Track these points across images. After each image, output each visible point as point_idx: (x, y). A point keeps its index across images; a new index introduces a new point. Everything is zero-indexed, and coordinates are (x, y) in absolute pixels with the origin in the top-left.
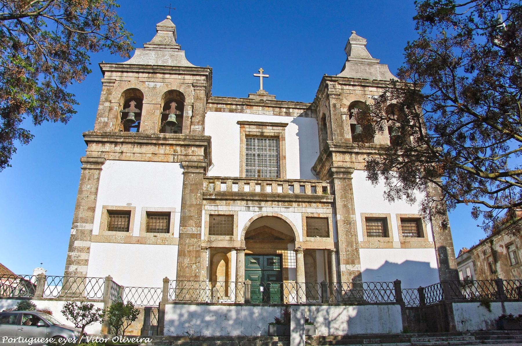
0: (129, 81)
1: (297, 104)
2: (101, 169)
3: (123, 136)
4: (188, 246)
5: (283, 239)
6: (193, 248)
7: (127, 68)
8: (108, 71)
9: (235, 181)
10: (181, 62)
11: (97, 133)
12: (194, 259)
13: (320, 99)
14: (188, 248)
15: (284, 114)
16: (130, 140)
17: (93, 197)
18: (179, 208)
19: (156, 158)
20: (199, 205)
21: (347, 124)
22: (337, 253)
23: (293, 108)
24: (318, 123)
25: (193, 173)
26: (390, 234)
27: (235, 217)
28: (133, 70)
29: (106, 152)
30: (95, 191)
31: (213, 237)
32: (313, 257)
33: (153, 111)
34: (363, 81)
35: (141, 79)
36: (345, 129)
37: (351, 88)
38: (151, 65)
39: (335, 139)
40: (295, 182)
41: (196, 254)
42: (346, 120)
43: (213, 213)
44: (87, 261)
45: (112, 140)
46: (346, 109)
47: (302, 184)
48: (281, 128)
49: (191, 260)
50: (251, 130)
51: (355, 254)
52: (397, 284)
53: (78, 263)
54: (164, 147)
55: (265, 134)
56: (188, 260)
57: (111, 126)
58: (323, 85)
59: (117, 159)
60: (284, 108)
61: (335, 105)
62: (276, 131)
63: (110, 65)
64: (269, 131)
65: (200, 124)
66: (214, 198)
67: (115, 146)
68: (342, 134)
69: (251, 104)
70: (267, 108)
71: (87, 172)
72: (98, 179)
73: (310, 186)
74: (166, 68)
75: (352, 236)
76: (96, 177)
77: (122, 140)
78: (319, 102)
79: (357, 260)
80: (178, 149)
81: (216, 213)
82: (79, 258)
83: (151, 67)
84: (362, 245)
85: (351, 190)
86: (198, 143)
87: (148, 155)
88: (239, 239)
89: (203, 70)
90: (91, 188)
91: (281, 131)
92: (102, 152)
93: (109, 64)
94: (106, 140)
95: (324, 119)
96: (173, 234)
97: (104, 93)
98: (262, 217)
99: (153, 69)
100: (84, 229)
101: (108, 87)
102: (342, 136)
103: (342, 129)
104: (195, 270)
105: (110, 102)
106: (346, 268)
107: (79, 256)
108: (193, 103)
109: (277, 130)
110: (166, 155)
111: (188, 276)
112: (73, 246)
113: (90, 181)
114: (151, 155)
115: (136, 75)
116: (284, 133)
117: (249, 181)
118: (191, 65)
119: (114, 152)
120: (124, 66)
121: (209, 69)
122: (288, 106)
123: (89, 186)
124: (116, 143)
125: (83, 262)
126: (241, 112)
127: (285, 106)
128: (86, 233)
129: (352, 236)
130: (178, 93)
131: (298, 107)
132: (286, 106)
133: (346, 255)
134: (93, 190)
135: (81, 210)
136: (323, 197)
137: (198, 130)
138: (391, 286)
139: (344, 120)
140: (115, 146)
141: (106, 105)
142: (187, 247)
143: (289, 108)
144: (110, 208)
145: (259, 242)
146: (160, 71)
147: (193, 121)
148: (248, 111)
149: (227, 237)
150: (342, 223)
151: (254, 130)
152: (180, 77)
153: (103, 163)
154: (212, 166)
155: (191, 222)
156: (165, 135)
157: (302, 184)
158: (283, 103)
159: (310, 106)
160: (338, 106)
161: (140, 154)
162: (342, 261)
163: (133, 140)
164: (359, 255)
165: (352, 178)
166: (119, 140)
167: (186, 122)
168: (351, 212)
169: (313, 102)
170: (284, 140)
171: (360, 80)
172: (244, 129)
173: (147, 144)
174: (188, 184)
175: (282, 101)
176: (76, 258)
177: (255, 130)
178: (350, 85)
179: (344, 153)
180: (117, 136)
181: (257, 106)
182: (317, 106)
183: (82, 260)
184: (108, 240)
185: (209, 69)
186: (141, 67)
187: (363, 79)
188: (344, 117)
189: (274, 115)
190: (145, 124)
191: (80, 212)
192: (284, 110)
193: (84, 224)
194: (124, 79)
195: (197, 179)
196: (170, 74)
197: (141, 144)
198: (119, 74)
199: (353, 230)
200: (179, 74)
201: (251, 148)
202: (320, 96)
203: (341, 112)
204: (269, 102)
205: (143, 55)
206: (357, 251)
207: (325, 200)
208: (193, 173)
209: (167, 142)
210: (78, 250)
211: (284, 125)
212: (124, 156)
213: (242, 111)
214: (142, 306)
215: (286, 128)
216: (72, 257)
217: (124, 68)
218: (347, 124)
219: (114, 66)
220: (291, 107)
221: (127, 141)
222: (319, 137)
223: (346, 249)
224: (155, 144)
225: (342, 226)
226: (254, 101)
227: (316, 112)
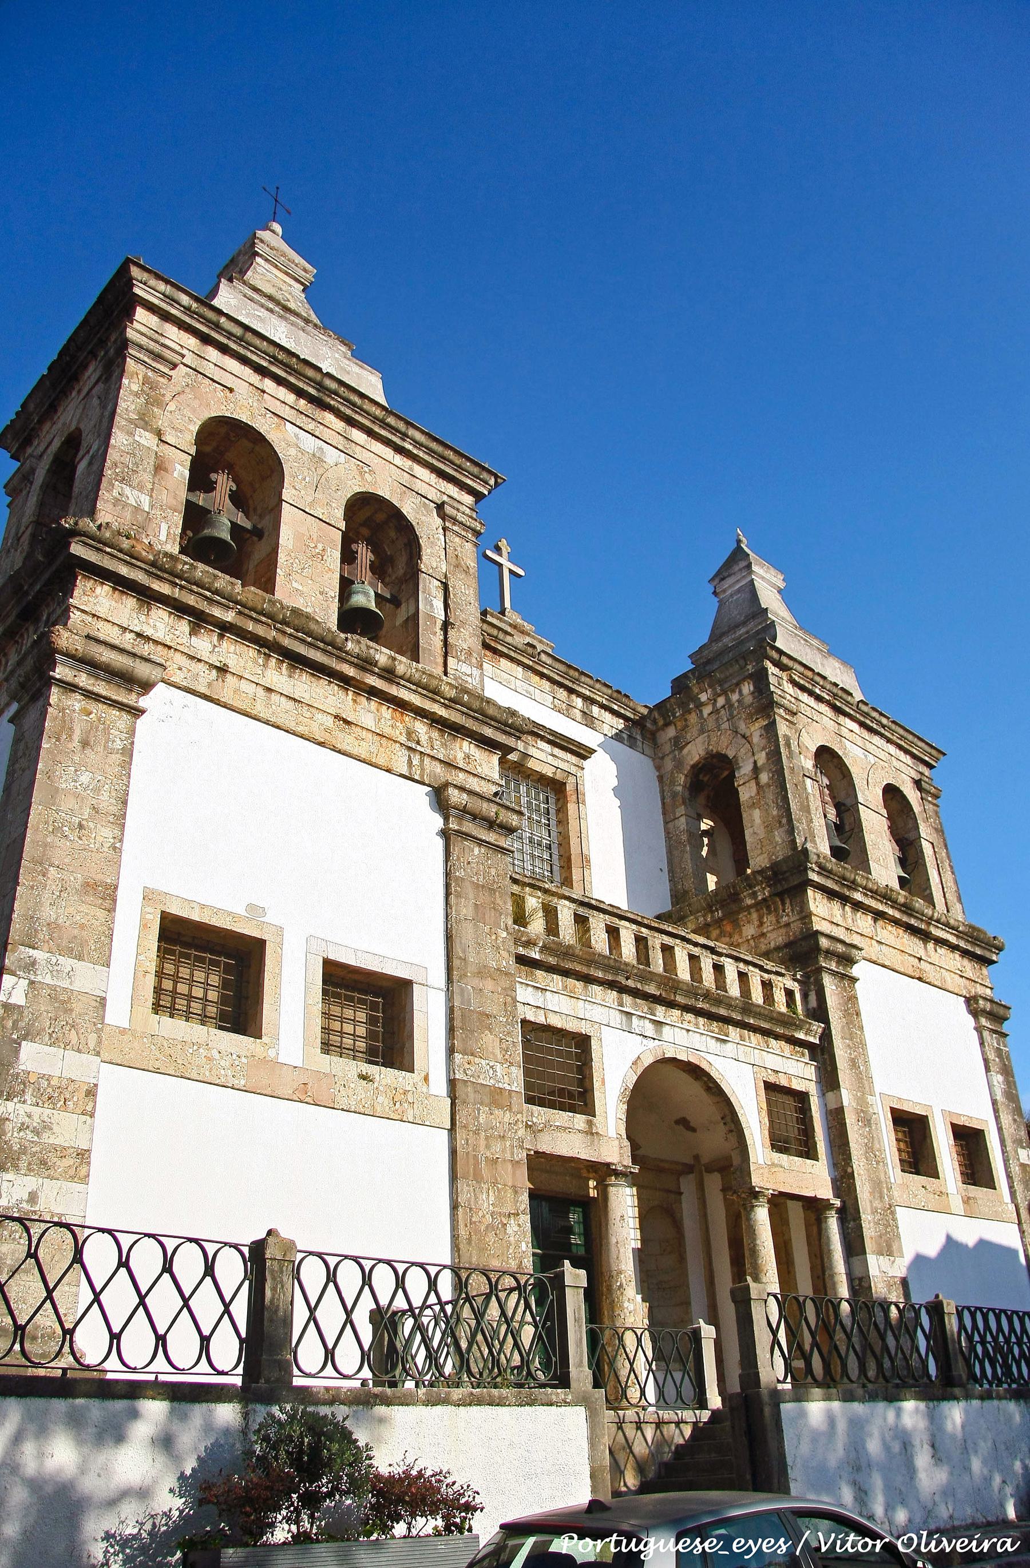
0: (231, 390)
1: (615, 695)
2: (137, 712)
3: (237, 603)
4: (487, 1138)
6: (504, 1151)
7: (230, 335)
11: (139, 548)
14: (488, 1147)
15: (578, 715)
16: (261, 631)
17: (106, 833)
18: (437, 975)
19: (346, 740)
23: (602, 706)
25: (481, 842)
28: (249, 355)
29: (156, 642)
30: (113, 809)
31: (540, 1114)
33: (320, 546)
34: (840, 693)
38: (318, 369)
43: (531, 1017)
44: (83, 1155)
45: (191, 600)
48: (574, 759)
49: (500, 1200)
53: (43, 1165)
54: (373, 705)
55: (531, 764)
59: (203, 690)
60: (579, 695)
63: (168, 289)
66: (537, 956)
67: (193, 632)
69: (500, 647)
70: (537, 678)
71: (77, 706)
72: (128, 752)
74: (367, 406)
76: (118, 745)
77: (229, 616)
80: (421, 728)
81: (541, 1019)
82: (48, 1138)
83: (318, 377)
86: (488, 732)
87: (319, 716)
88: (612, 1133)
89: (476, 470)
90: (97, 790)
92: (139, 635)
93: (167, 282)
94: (165, 589)
97: (135, 388)
99: (320, 386)
100: (65, 984)
101: (150, 374)
104: (518, 1246)
105: (159, 434)
107: (47, 1127)
110: (384, 741)
112: (10, 1065)
113: (91, 756)
114: (331, 719)
117: (653, 924)
119: (192, 658)
120: (223, 320)
121: (496, 477)
122: (592, 696)
123: (85, 778)
124: (199, 620)
125: (68, 1162)
127: (583, 691)
128: (77, 1007)
131: (616, 707)
132: (588, 693)
134: (107, 801)
135: (53, 886)
140: (193, 632)
141: (143, 441)
142: (483, 1143)
143: (593, 702)
146: (342, 408)
149: (579, 1120)
152: (399, 460)
153: (146, 687)
156: (394, 659)
158: (583, 679)
159: (643, 718)
161: (291, 703)
163: (271, 634)
166: (217, 612)
171: (835, 690)
173: (319, 670)
174: (467, 884)
175: (582, 673)
176: (30, 1136)
180: (216, 592)
181: (512, 659)
183: (62, 1152)
185: (496, 477)
186: (281, 356)
187: (842, 689)
190: (295, 585)
191: (47, 895)
192: (579, 702)
193: (67, 963)
194: (210, 370)
195: (493, 871)
196: (370, 433)
197: (296, 661)
198: (192, 342)
200: (399, 450)
204: (549, 661)
208: (481, 842)
209: (393, 690)
210: (38, 1092)
211: (582, 752)
212: (227, 690)
216: (9, 1126)
217: (217, 327)
219: (185, 299)
220: (599, 699)
221: (251, 626)
224: (345, 682)
226: (509, 639)
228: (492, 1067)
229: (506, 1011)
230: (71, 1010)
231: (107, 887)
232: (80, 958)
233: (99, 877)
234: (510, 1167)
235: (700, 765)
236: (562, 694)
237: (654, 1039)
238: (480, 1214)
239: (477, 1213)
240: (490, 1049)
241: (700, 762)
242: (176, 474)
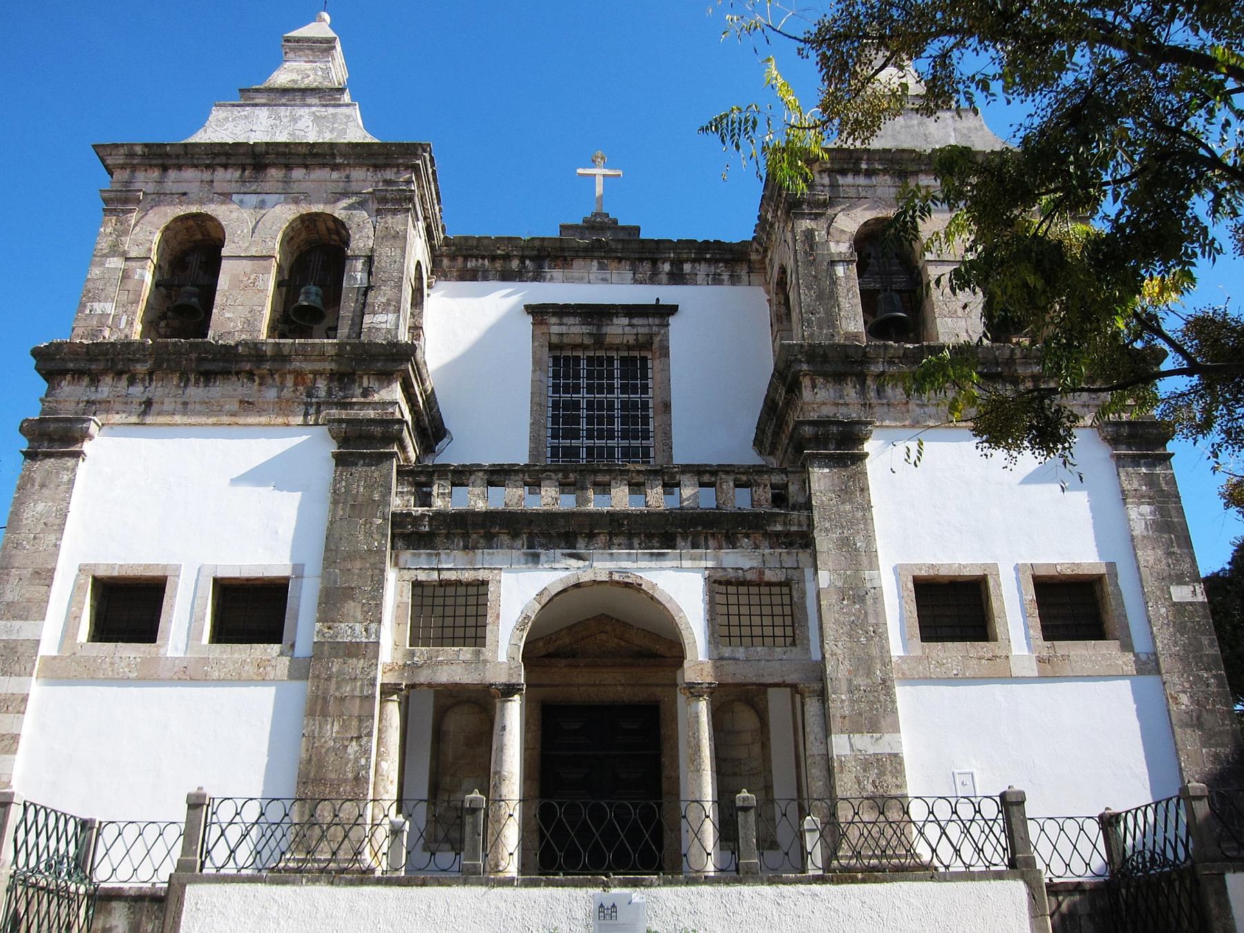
0: (185, 194)
5: (662, 656)
6: (353, 690)
8: (123, 167)
9: (495, 478)
10: (345, 133)
12: (355, 723)
13: (772, 225)
14: (337, 689)
15: (664, 277)
20: (376, 552)
21: (848, 291)
22: (823, 695)
23: (694, 261)
24: (769, 301)
26: (999, 630)
27: (491, 588)
29: (100, 403)
32: (757, 712)
33: (253, 277)
35: (218, 186)
36: (845, 303)
37: (861, 180)
39: (811, 335)
40: (683, 472)
41: (361, 706)
42: (847, 277)
46: (847, 245)
47: (706, 478)
48: (657, 321)
49: (344, 727)
50: (564, 329)
51: (882, 698)
52: (1011, 804)
56: (336, 728)
57: (122, 326)
61: (809, 234)
62: (641, 330)
64: (618, 329)
65: (392, 308)
66: (427, 529)
68: (831, 320)
73: (731, 484)
75: (869, 639)
78: (769, 234)
79: (889, 720)
84: (905, 667)
85: (862, 490)
88: (502, 657)
91: (655, 329)
92: (88, 402)
95: (782, 284)
96: (293, 646)
97: (109, 230)
98: (578, 586)
100: (14, 637)
102: (834, 326)
103: (833, 306)
104: (357, 760)
106: (851, 746)
108: (372, 250)
109: (643, 325)
111: (332, 780)
113: (46, 492)
115: (207, 175)
116: (666, 336)
118: (376, 141)
126: (534, 279)
128: (21, 650)
129: (869, 639)
130: (331, 224)
133: (852, 701)
136: (772, 517)
137: (384, 326)
138: (990, 809)
139: (838, 278)
141: (112, 266)
142: (333, 686)
144: (101, 573)
145: (585, 666)
147: (369, 300)
148: (557, 273)
149: (466, 653)
150: (834, 598)
151: (575, 329)
152: (335, 175)
154: (445, 440)
155: (352, 608)
157: (706, 478)
160: (820, 236)
162: (835, 724)
164: (893, 702)
165: (867, 455)
167: (348, 306)
168: (864, 560)
169: (754, 238)
170: (667, 355)
172: (544, 329)
177: (577, 330)
178: (857, 172)
179: (839, 378)
182: (766, 250)
184: (90, 675)
188: (840, 270)
189: (636, 281)
190: (227, 315)
193: (17, 624)
196: (306, 167)
199: (871, 620)
201: (576, 389)
202: (769, 216)
203: (831, 254)
205: (234, 120)
206: (889, 693)
207: (779, 528)
211: (665, 312)
213: (538, 277)
214: (154, 884)
215: (672, 320)
218: (848, 291)
222: (774, 342)
223: (850, 681)
225: (837, 608)
227: (765, 268)
228: (351, 628)
229: (372, 581)
230: (16, 652)
231: (49, 570)
232: (26, 619)
233: (45, 566)
234: (358, 701)
236: (647, 266)
238: (323, 740)
239: (319, 740)
240: (351, 614)
242: (136, 277)
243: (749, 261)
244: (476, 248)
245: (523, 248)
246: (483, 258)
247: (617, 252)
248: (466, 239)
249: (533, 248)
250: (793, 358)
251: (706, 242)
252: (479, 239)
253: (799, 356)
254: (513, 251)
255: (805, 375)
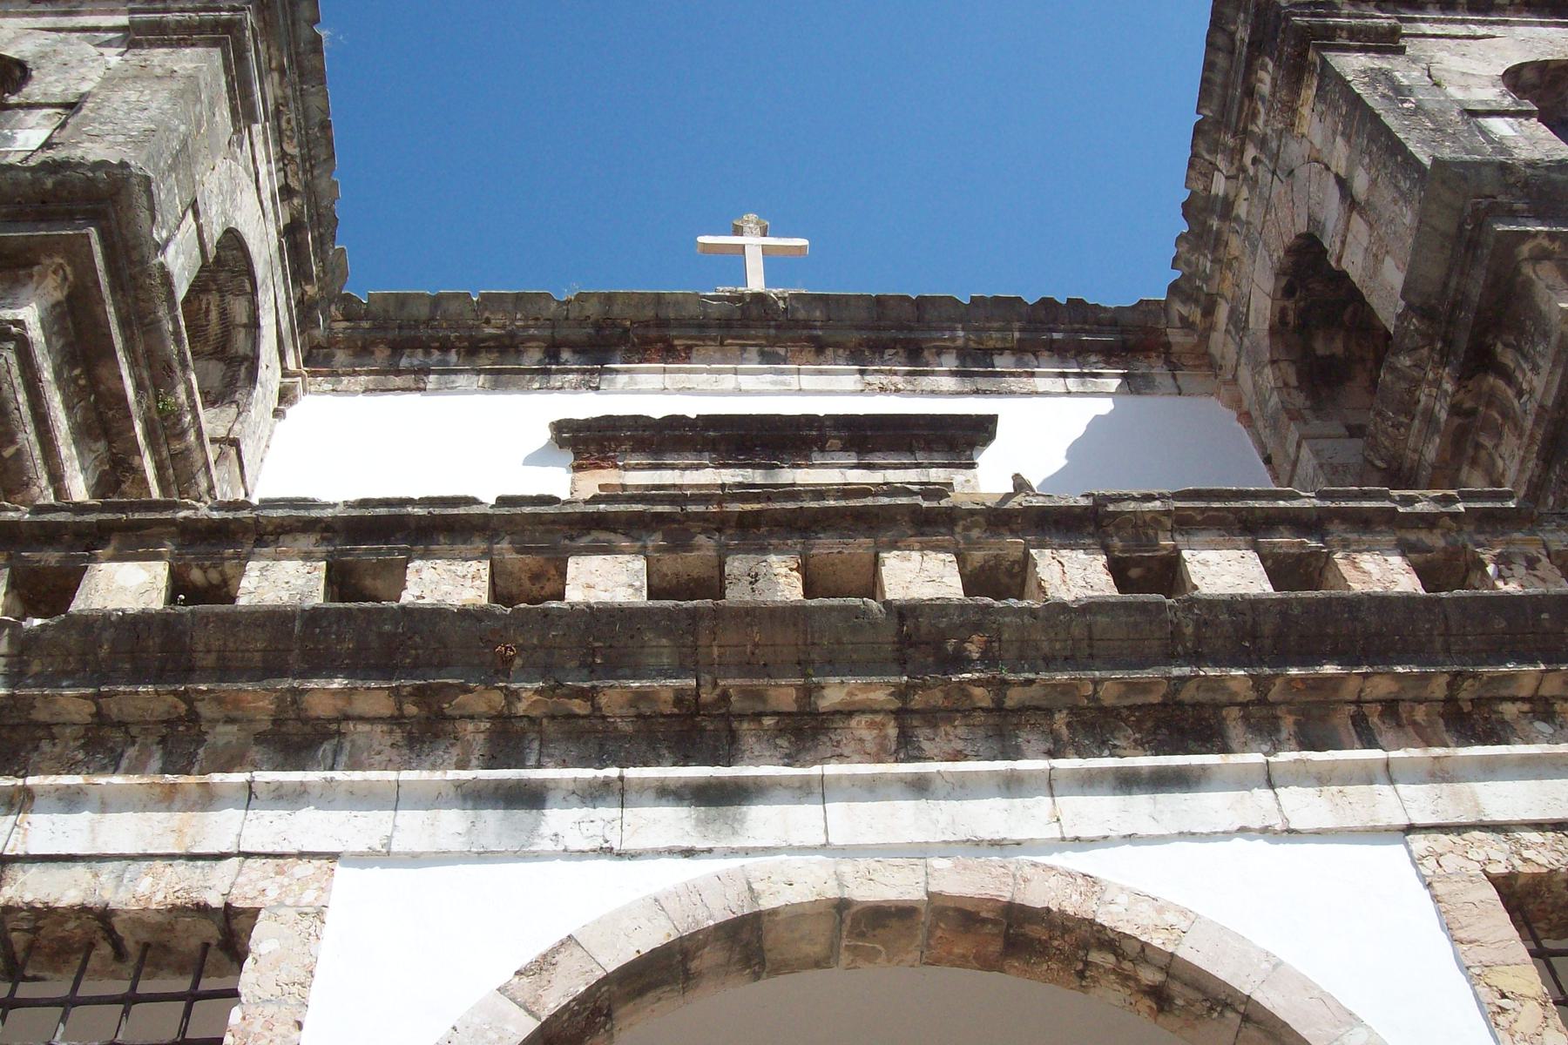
27: (264, 941)
40: (1185, 524)
58: (1231, 52)
169: (1174, 288)
235: (1291, 317)
237: (689, 853)
241: (1283, 311)
243: (1168, 345)
244: (427, 323)
245: (553, 323)
246: (445, 347)
247: (815, 328)
248: (402, 300)
249: (582, 322)
250: (1485, 203)
251: (1047, 303)
252: (437, 301)
253: (1501, 199)
254: (527, 327)
255: (1540, 256)
